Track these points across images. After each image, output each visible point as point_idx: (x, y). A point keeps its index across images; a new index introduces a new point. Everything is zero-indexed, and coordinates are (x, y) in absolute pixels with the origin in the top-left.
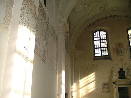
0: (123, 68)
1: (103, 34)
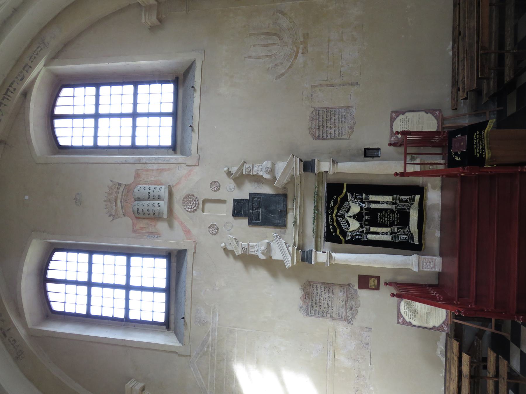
0: (234, 200)
1: (63, 264)
